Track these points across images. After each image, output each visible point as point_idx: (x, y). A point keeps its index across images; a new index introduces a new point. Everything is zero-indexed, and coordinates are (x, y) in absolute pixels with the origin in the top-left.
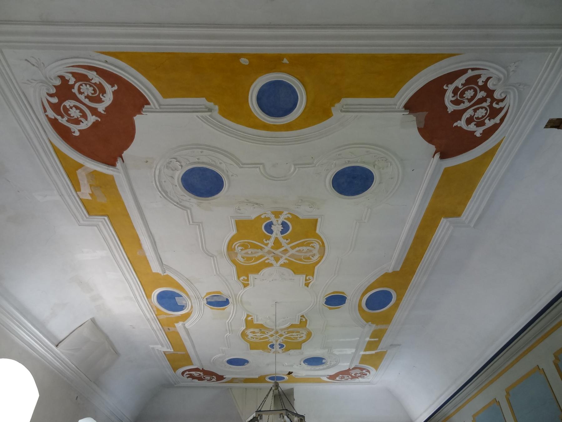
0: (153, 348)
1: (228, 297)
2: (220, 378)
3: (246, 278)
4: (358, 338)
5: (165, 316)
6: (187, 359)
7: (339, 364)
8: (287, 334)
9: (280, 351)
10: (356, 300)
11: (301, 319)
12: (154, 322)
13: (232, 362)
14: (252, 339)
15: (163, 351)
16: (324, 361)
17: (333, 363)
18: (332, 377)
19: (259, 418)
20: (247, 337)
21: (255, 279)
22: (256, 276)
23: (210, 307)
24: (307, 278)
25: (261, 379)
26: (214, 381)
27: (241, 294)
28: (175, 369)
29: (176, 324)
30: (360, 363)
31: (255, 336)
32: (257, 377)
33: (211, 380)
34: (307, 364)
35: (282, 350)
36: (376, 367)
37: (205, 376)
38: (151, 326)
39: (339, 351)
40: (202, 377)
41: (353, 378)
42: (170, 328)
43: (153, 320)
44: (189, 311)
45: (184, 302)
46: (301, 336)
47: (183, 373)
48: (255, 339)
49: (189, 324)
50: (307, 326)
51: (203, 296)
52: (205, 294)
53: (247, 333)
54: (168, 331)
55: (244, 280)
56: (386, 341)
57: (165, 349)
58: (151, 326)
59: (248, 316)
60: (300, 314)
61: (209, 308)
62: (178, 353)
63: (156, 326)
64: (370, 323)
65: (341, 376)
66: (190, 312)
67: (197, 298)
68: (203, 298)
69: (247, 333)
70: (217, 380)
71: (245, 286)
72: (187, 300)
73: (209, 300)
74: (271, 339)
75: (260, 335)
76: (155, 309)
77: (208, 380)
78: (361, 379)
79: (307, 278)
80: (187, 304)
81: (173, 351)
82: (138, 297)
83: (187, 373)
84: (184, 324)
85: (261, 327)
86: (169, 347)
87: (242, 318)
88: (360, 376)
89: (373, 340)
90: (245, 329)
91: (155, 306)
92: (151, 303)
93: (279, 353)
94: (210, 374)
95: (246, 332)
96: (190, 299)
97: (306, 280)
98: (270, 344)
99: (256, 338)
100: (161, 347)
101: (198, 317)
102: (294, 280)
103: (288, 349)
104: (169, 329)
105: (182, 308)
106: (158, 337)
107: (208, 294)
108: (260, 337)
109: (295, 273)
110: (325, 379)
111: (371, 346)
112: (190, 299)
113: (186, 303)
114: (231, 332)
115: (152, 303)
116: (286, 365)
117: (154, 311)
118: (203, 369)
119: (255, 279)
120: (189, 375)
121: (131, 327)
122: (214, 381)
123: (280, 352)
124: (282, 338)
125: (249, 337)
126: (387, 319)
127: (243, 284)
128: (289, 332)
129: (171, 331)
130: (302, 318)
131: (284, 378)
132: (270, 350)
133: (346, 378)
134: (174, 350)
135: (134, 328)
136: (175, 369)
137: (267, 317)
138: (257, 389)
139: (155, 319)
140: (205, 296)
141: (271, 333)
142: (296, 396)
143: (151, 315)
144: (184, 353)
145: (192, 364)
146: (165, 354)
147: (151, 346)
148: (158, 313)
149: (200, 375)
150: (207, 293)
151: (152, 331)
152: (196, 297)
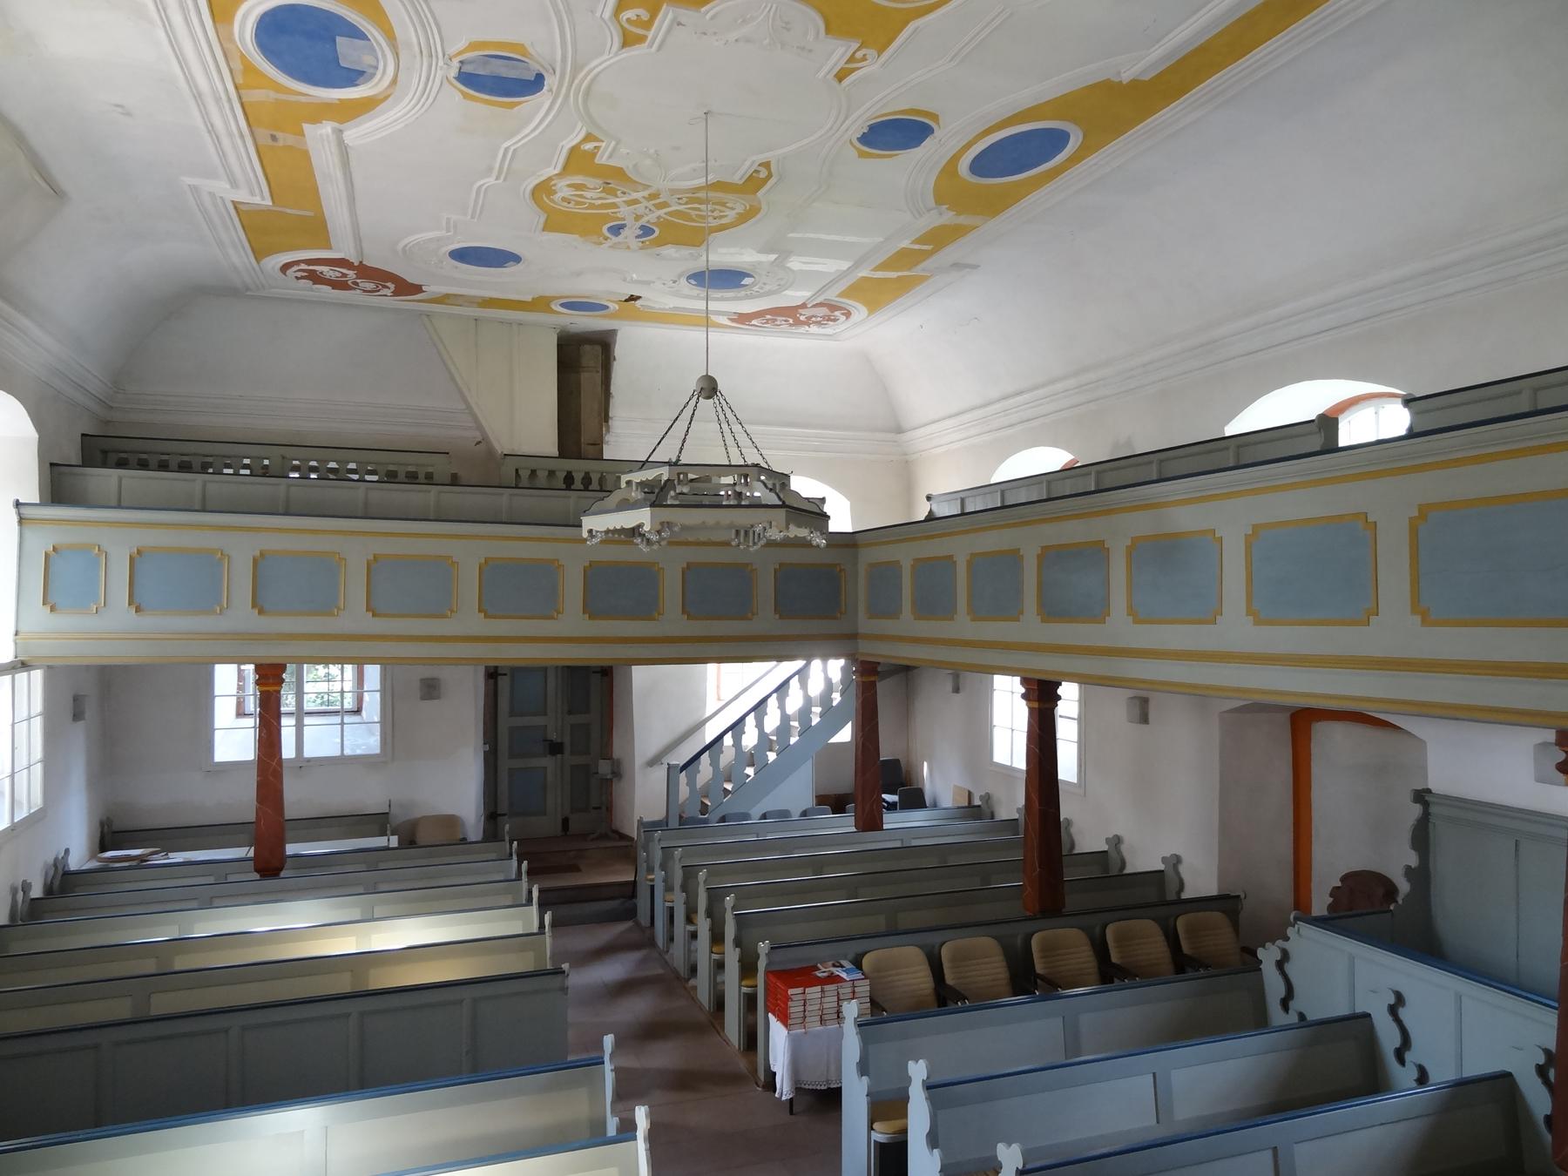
0: (195, 190)
1: (547, 71)
2: (406, 288)
3: (645, 16)
4: (881, 239)
5: (272, 95)
6: (317, 230)
7: (785, 292)
8: (686, 203)
9: (635, 244)
10: (954, 145)
11: (756, 171)
12: (221, 109)
13: (462, 255)
14: (565, 204)
15: (233, 201)
16: (746, 281)
17: (767, 288)
18: (743, 319)
19: (676, 482)
20: (548, 198)
21: (679, 24)
22: (686, 15)
23: (462, 92)
24: (859, 55)
25: (541, 304)
26: (386, 296)
27: (595, 72)
28: (259, 254)
29: (307, 127)
30: (841, 295)
31: (581, 196)
32: (529, 298)
33: (379, 291)
34: (694, 282)
35: (643, 242)
36: (874, 306)
37: (358, 281)
38: (205, 115)
39: (804, 263)
40: (349, 283)
41: (798, 323)
42: (279, 134)
43: (218, 100)
44: (380, 93)
45: (368, 60)
46: (722, 214)
47: (285, 268)
48: (570, 205)
49: (358, 133)
50: (760, 194)
51: (451, 51)
52: (462, 45)
53: (555, 185)
54: (270, 142)
55: (638, 22)
56: (950, 253)
57: (242, 196)
58: (205, 115)
59: (589, 138)
60: (762, 158)
61: (458, 97)
62: (289, 211)
63: (229, 121)
64: (947, 206)
65: (768, 317)
66: (381, 97)
67: (425, 52)
68: (450, 59)
69: (555, 185)
70: (396, 293)
71: (628, 40)
72: (384, 56)
73: (468, 69)
74: (625, 212)
75: (595, 196)
76: (237, 65)
77: (365, 291)
78: (814, 329)
79: (859, 55)
80: (376, 68)
81: (271, 204)
82: (169, 11)
83: (303, 266)
84: (341, 131)
85: (614, 177)
86: (257, 191)
87: (564, 142)
88: (818, 323)
89: (916, 247)
90: (556, 175)
91: (242, 56)
92: (225, 39)
93: (628, 248)
94: (365, 271)
95: (553, 182)
96: (396, 56)
97: (852, 59)
98: (612, 224)
99: (578, 203)
100: (228, 186)
101: (405, 115)
102: (810, 51)
103: (661, 242)
104: (274, 138)
105: (353, 77)
106: (223, 156)
107: (473, 46)
108: (593, 201)
109: (828, 30)
110: (724, 320)
111: (904, 259)
112: (396, 56)
113: (374, 63)
114: (502, 178)
115: (232, 40)
116: (632, 278)
117: (231, 71)
118: (361, 262)
119: (679, 24)
120: (306, 274)
121: (120, 110)
122: (386, 296)
123: (631, 247)
124: (661, 212)
125: (557, 197)
126: (994, 205)
127: (624, 35)
128: (691, 201)
129: (281, 143)
130: (761, 168)
131: (607, 307)
132: (606, 239)
133: (778, 323)
134: (273, 202)
135: (128, 114)
136: (259, 254)
137: (652, 151)
138: (511, 324)
139: (229, 100)
140: (460, 53)
141: (635, 195)
142: (619, 350)
143: (213, 81)
144: (312, 214)
145: (330, 248)
146: (236, 208)
147: (189, 180)
148: (246, 79)
149: (344, 275)
150: (470, 44)
151: (207, 135)
152: (421, 52)
